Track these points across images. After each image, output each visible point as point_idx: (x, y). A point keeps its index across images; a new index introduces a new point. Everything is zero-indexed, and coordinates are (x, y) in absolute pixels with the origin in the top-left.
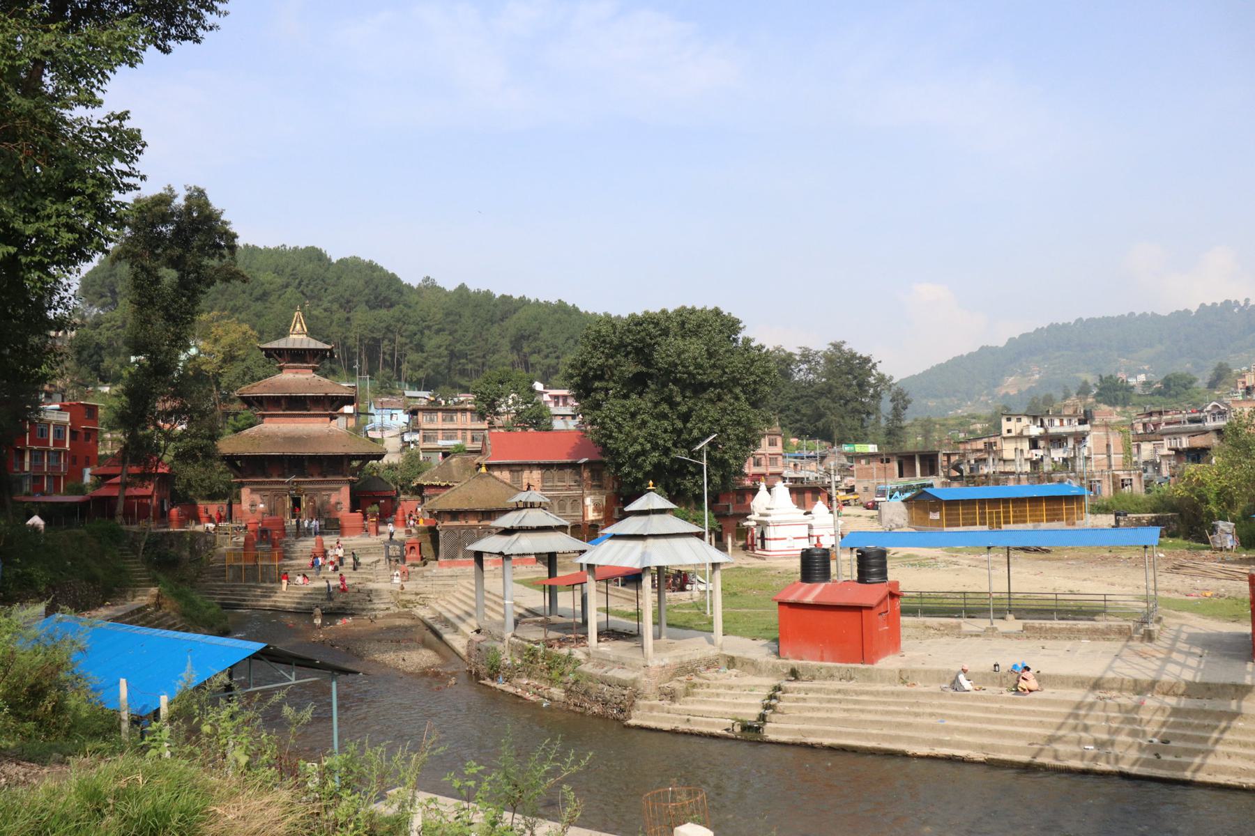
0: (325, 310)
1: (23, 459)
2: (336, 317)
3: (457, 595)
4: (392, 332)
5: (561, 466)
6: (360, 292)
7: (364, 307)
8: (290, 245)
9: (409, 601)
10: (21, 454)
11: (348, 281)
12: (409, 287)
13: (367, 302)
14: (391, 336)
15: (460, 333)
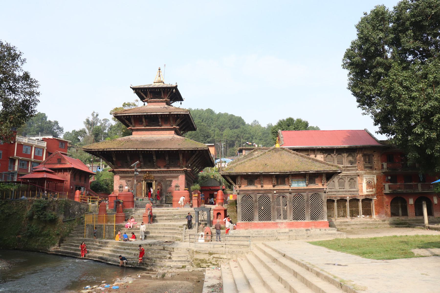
0: (212, 131)
1: (14, 164)
2: (215, 133)
3: (250, 257)
4: (239, 137)
5: (340, 151)
6: (227, 123)
7: (228, 129)
8: (200, 108)
9: (203, 261)
10: (13, 161)
11: (221, 119)
12: (248, 125)
13: (229, 128)
14: (239, 139)
15: (269, 140)
